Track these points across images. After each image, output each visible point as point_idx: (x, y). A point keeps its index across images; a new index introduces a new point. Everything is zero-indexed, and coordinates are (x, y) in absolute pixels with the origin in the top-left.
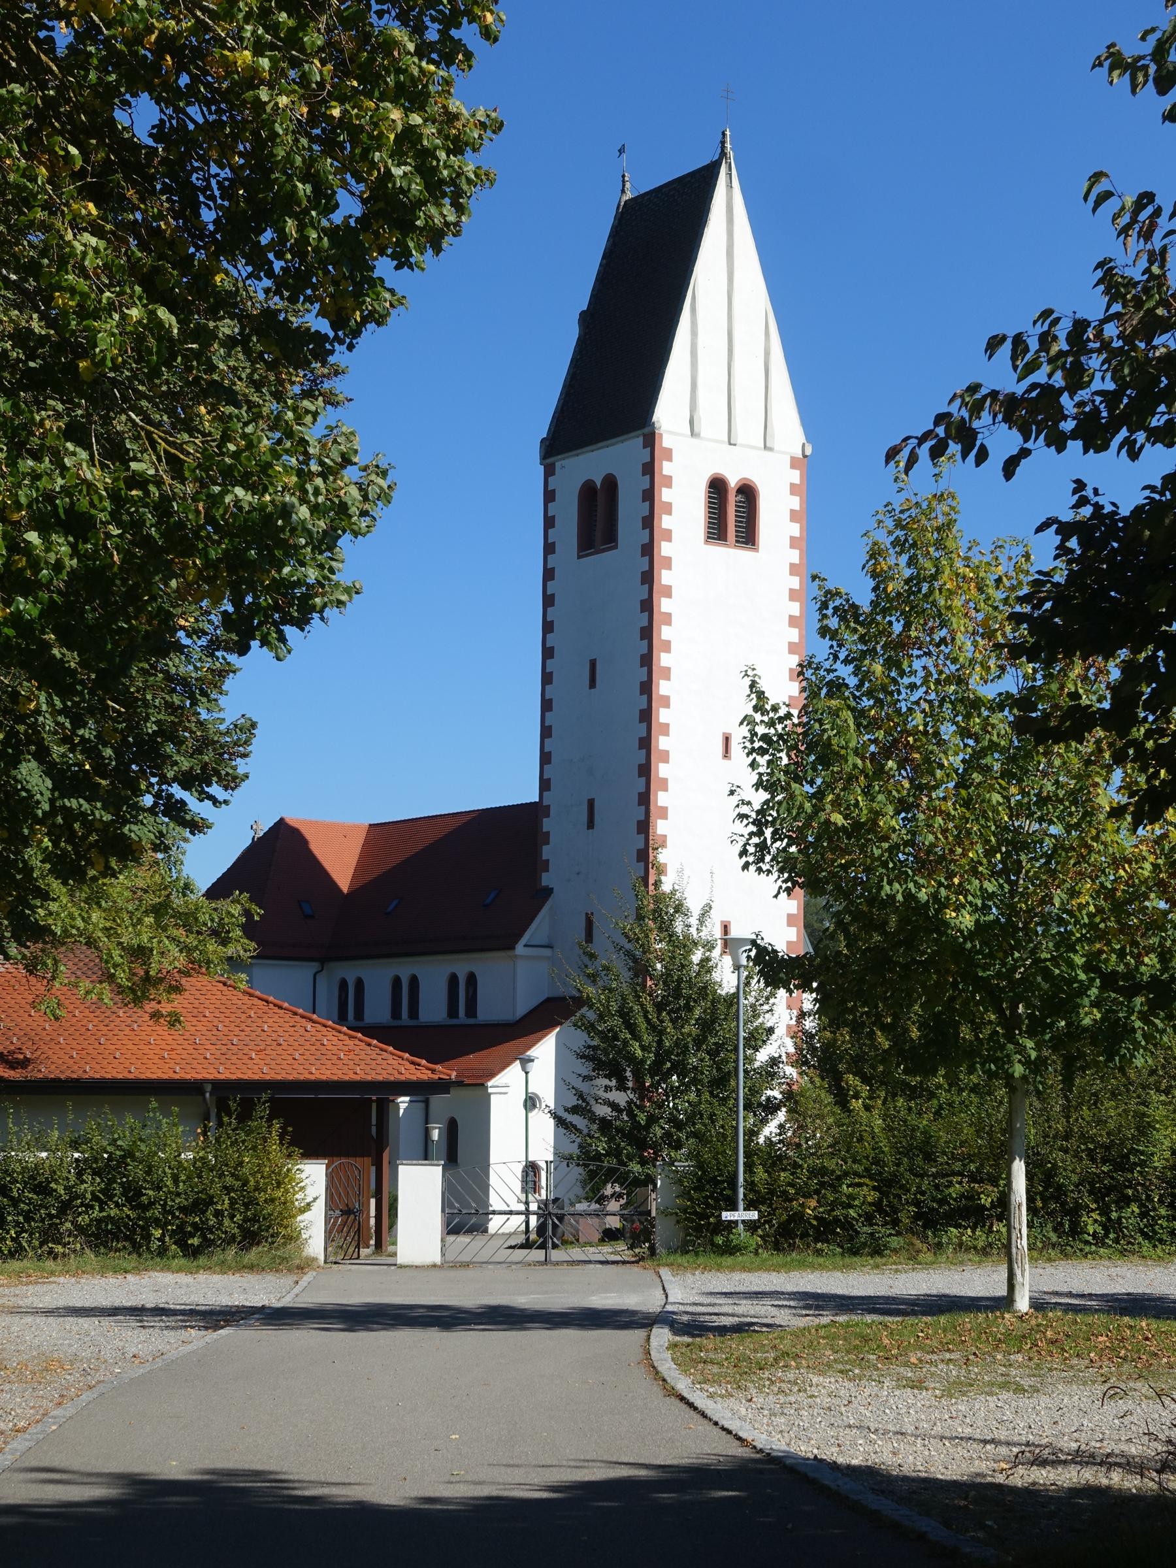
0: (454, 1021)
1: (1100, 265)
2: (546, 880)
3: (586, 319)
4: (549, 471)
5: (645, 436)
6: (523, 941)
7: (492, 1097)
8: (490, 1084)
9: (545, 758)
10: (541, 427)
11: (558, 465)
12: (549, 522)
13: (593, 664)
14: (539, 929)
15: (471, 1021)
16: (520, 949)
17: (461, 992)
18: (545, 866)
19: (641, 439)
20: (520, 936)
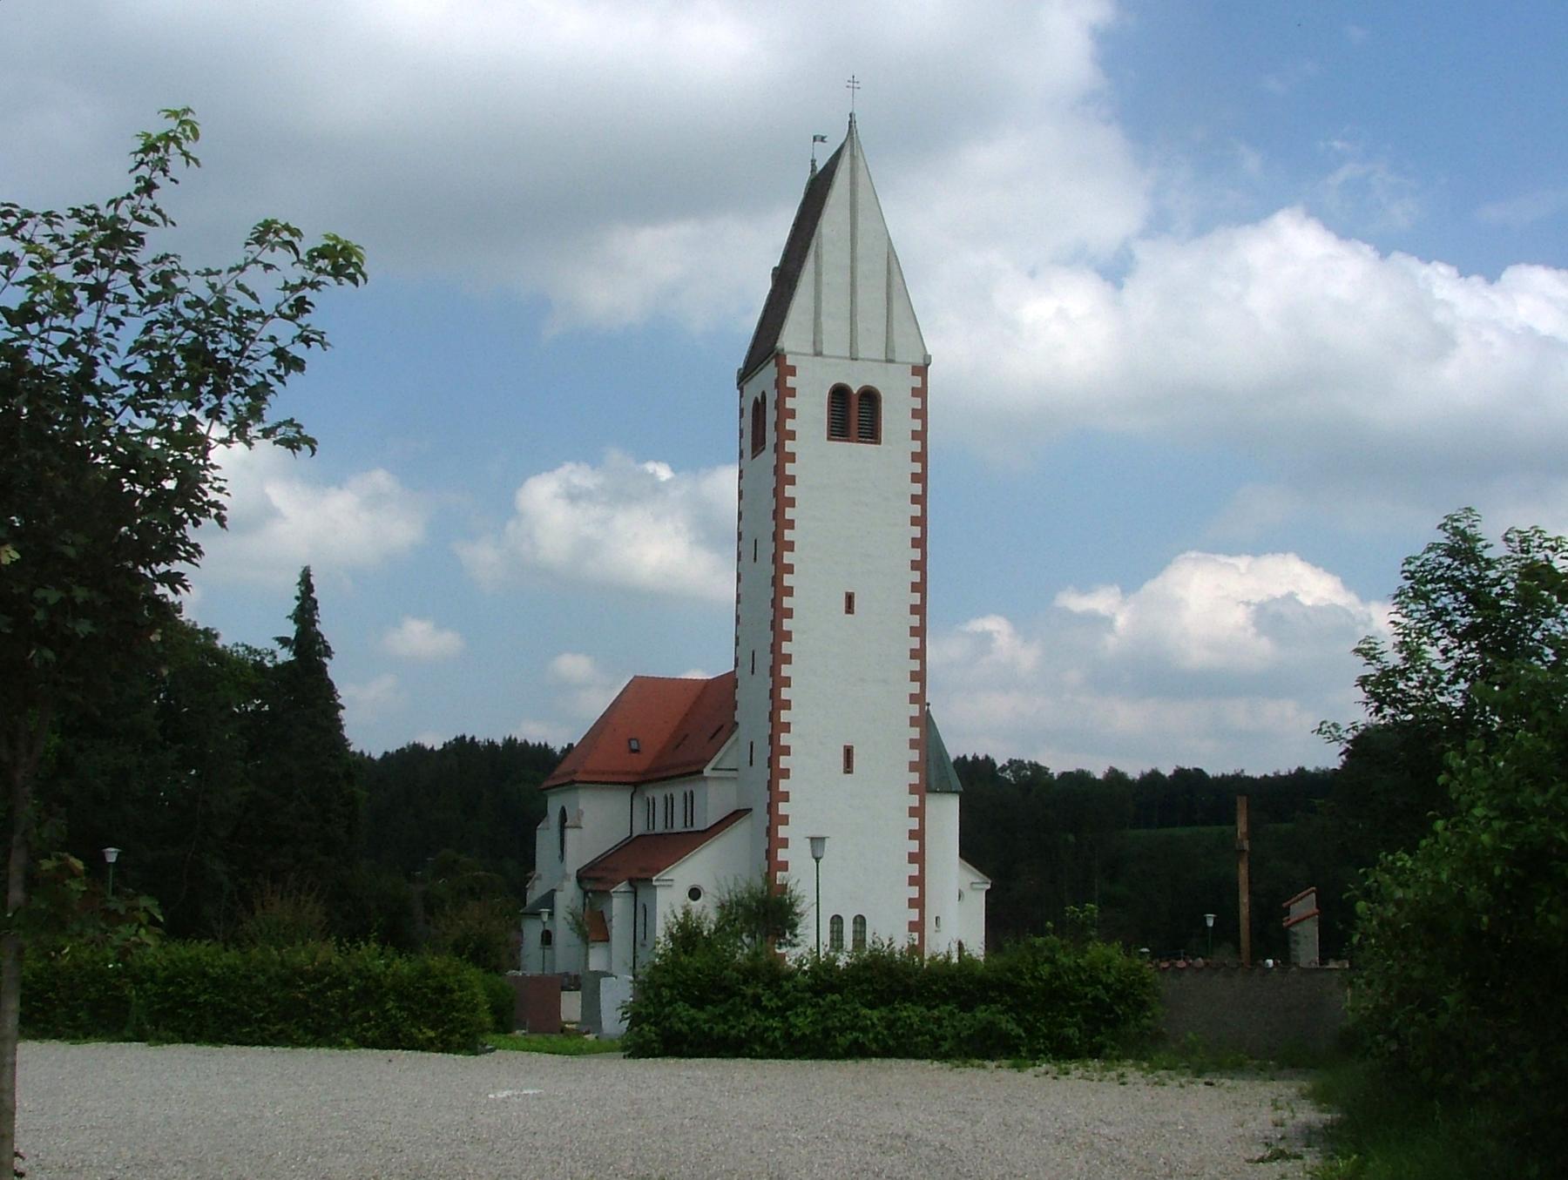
4: (741, 390)
6: (710, 766)
7: (659, 891)
16: (707, 771)
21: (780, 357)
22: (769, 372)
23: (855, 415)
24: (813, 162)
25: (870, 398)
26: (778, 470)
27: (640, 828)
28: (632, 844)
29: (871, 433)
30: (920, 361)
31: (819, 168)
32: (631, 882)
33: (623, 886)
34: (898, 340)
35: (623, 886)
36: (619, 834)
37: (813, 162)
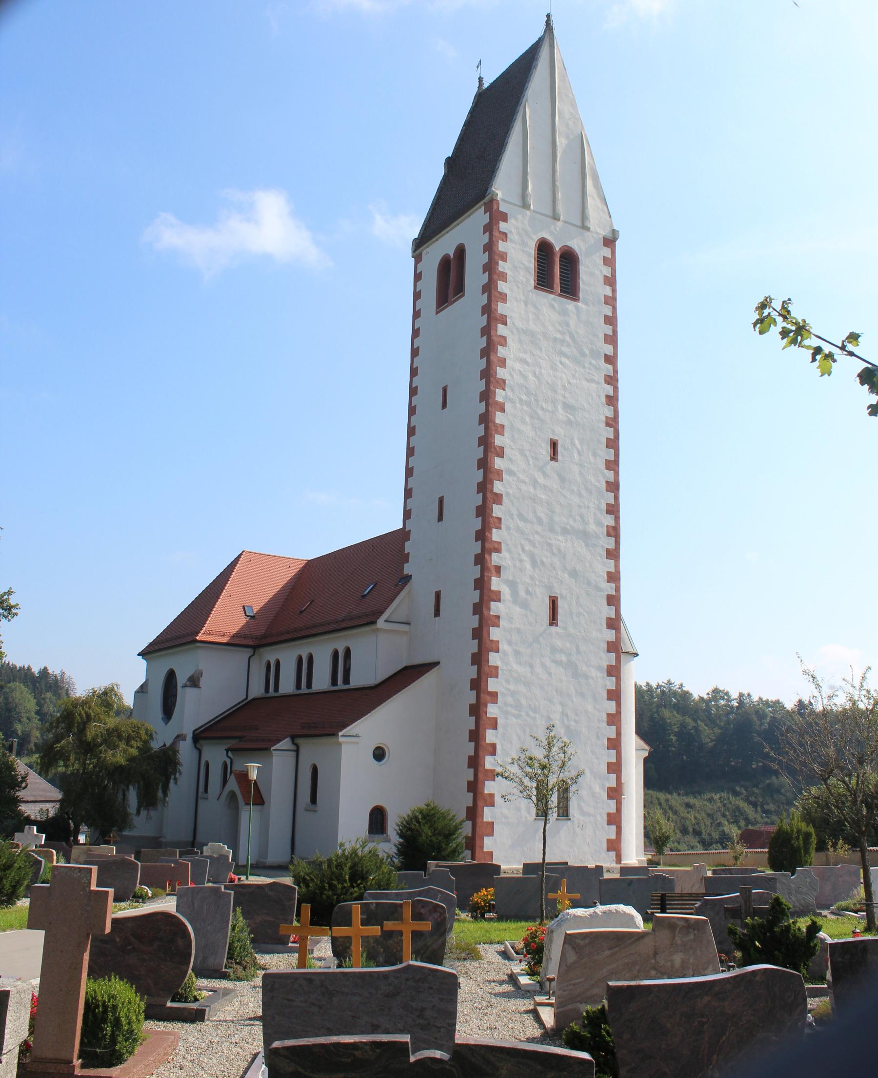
1: (762, 324)
2: (407, 569)
3: (450, 163)
4: (418, 258)
5: (485, 204)
6: (385, 616)
8: (340, 734)
9: (409, 472)
12: (417, 296)
14: (397, 608)
15: (346, 687)
16: (381, 623)
18: (406, 558)
19: (483, 208)
20: (381, 613)
22: (478, 217)
23: (557, 270)
24: (480, 80)
25: (570, 259)
26: (488, 310)
29: (570, 288)
30: (610, 236)
31: (486, 85)
32: (293, 738)
33: (285, 744)
35: (285, 744)
36: (235, 698)
37: (480, 80)
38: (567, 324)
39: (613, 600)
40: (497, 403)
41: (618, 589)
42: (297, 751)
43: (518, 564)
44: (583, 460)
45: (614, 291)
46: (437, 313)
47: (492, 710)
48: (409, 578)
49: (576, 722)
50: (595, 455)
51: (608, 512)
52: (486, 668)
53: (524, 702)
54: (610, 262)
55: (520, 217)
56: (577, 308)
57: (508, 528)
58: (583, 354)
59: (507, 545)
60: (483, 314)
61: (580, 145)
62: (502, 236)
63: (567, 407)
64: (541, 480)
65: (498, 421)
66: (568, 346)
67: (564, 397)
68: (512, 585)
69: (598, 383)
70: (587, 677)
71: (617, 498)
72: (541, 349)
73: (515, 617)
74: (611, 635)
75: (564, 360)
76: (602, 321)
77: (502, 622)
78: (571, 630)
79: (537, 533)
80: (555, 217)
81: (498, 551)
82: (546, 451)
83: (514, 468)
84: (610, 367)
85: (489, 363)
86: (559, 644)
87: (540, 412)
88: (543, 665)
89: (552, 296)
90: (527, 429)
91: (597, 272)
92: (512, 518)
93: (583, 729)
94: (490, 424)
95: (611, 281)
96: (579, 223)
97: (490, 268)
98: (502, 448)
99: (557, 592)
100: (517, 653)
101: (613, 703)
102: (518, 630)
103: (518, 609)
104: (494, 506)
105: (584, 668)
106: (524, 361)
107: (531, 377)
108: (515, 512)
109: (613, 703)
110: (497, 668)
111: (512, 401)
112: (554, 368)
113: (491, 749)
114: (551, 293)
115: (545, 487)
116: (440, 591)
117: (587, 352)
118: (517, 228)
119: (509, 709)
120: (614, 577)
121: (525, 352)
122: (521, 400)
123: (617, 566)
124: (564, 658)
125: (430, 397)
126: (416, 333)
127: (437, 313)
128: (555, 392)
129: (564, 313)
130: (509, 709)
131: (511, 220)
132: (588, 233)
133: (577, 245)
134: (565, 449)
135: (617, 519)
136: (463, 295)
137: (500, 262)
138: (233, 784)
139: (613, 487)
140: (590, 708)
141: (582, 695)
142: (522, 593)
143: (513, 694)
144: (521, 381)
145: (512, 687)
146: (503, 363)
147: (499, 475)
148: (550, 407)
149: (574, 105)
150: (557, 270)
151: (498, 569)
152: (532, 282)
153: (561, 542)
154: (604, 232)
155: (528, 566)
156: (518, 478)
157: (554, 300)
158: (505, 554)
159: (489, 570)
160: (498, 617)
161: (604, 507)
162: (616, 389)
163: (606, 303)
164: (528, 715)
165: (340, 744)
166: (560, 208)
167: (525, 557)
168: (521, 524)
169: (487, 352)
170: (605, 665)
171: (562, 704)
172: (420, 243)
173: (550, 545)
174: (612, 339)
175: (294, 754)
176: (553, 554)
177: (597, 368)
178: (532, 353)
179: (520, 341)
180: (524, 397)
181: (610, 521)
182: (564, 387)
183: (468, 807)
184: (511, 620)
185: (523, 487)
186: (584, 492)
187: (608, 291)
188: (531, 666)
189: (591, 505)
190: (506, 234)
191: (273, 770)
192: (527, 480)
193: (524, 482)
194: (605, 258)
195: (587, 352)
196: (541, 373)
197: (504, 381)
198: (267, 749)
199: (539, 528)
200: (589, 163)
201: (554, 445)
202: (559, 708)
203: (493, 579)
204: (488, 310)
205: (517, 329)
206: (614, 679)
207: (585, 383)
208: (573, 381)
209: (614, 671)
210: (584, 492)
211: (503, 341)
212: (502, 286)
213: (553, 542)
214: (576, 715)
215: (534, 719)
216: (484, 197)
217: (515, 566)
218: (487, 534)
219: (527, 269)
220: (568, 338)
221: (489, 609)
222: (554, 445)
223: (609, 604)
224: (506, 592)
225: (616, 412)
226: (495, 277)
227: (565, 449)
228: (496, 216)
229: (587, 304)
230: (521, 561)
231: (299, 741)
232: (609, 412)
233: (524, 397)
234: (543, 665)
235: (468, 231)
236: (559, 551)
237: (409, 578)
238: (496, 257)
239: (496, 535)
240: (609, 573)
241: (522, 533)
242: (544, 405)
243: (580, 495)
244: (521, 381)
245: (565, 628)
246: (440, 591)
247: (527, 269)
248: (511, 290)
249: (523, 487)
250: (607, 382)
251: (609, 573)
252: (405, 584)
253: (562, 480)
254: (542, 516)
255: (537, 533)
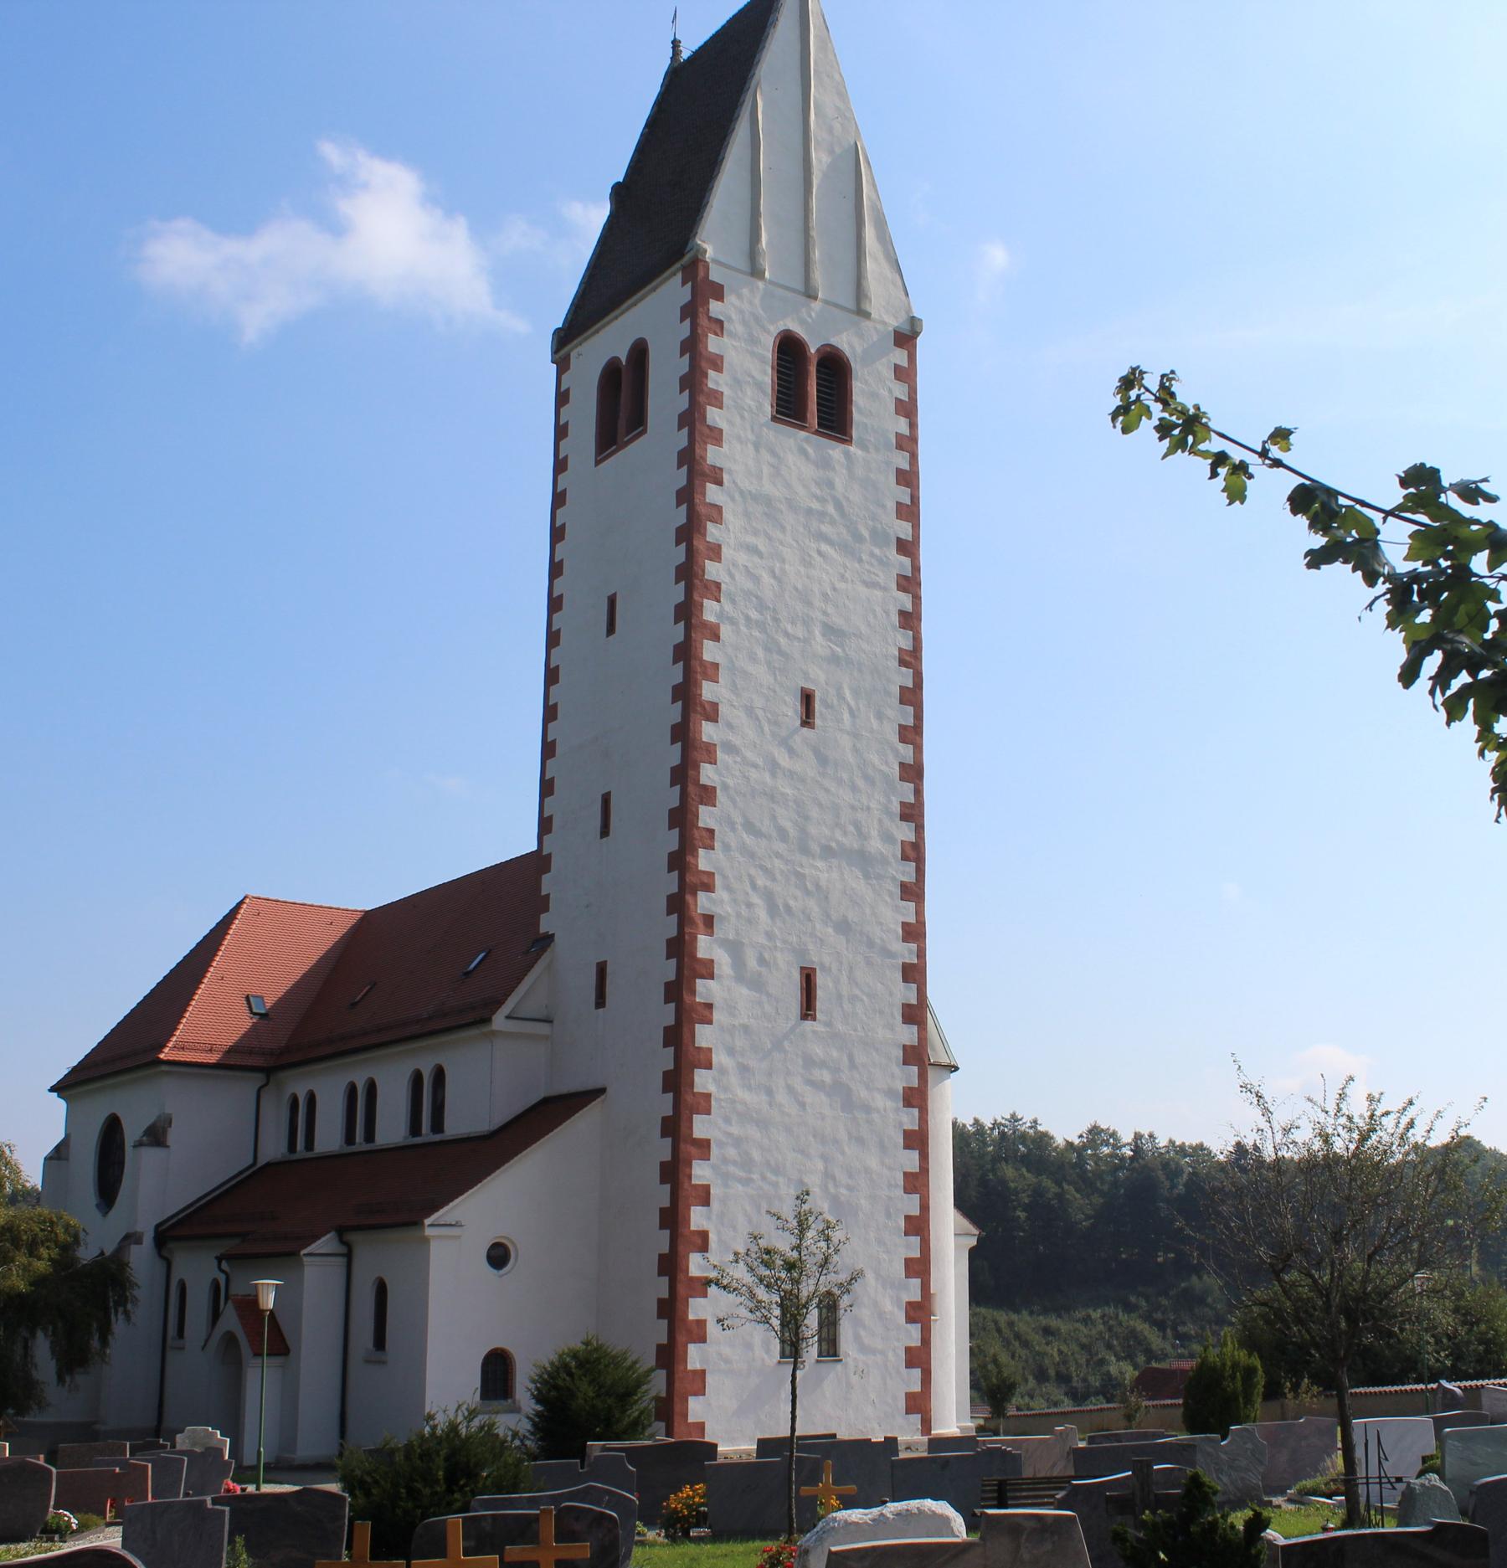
0: (418, 1140)
2: (546, 923)
3: (620, 193)
4: (562, 365)
5: (684, 268)
7: (434, 1247)
8: (427, 1222)
9: (548, 750)
10: (557, 318)
11: (573, 355)
12: (561, 432)
13: (612, 601)
14: (529, 993)
15: (437, 1138)
16: (499, 1021)
17: (428, 1094)
18: (543, 904)
19: (679, 276)
20: (499, 1003)
21: (694, 270)
22: (672, 291)
23: (813, 389)
24: (675, 44)
25: (835, 368)
26: (688, 457)
27: (274, 1148)
28: (256, 1180)
29: (835, 421)
30: (906, 329)
31: (685, 55)
32: (341, 1232)
34: (873, 285)
37: (675, 44)
38: (830, 485)
39: (914, 973)
40: (706, 625)
41: (921, 954)
42: (349, 1256)
43: (744, 911)
44: (859, 727)
45: (913, 426)
46: (598, 463)
47: (701, 1172)
48: (549, 938)
49: (850, 1188)
50: (880, 716)
51: (905, 817)
52: (689, 1098)
53: (756, 1155)
54: (906, 375)
55: (745, 291)
56: (847, 455)
57: (727, 848)
58: (859, 538)
59: (725, 877)
60: (680, 466)
61: (853, 164)
62: (714, 326)
63: (830, 631)
64: (783, 760)
65: (707, 657)
66: (833, 523)
67: (825, 613)
68: (735, 949)
69: (885, 589)
70: (867, 1109)
71: (918, 792)
72: (783, 529)
73: (738, 1006)
74: (909, 1034)
75: (825, 547)
76: (893, 478)
77: (716, 1015)
78: (840, 1027)
79: (778, 855)
80: (810, 294)
81: (709, 888)
82: (791, 710)
83: (736, 740)
84: (907, 561)
85: (690, 553)
86: (818, 1051)
87: (783, 641)
88: (791, 1090)
89: (803, 434)
90: (760, 672)
91: (885, 393)
92: (733, 829)
93: (863, 1201)
94: (693, 662)
95: (907, 409)
96: (851, 305)
97: (692, 382)
98: (715, 706)
99: (814, 958)
100: (744, 1069)
101: (915, 1155)
102: (746, 1029)
103: (745, 991)
104: (702, 808)
105: (864, 1094)
106: (753, 550)
107: (766, 578)
108: (739, 820)
109: (915, 1155)
110: (708, 1096)
111: (733, 622)
112: (807, 563)
113: (699, 1242)
114: (802, 428)
115: (791, 774)
116: (605, 962)
117: (866, 533)
118: (741, 312)
119: (732, 1168)
120: (914, 933)
121: (756, 533)
122: (748, 618)
123: (920, 913)
124: (827, 1077)
125: (585, 614)
126: (559, 499)
127: (598, 463)
128: (809, 604)
129: (825, 464)
130: (732, 1168)
131: (730, 298)
132: (867, 323)
133: (847, 343)
134: (828, 706)
135: (920, 829)
136: (644, 432)
137: (711, 373)
138: (230, 1320)
139: (913, 772)
140: (873, 1162)
141: (860, 1141)
142: (752, 963)
143: (738, 1142)
144: (749, 585)
145: (735, 1130)
146: (715, 552)
147: (710, 753)
148: (799, 631)
149: (842, 95)
150: (813, 389)
151: (709, 920)
152: (768, 409)
153: (821, 871)
154: (894, 322)
155: (762, 914)
156: (744, 758)
157: (807, 440)
158: (720, 893)
159: (693, 922)
160: (710, 1006)
161: (896, 808)
162: (917, 599)
163: (900, 447)
164: (764, 1178)
165: (426, 1241)
166: (818, 277)
167: (756, 899)
168: (749, 840)
169: (688, 533)
170: (899, 1086)
171: (825, 1159)
172: (566, 339)
173: (801, 876)
174: (910, 512)
175: (342, 1260)
176: (808, 893)
177: (884, 563)
178: (770, 539)
179: (747, 515)
180: (754, 615)
181: (906, 832)
182: (825, 595)
183: (659, 1346)
184: (732, 1010)
185: (753, 774)
186: (861, 783)
187: (902, 426)
188: (769, 1092)
189: (873, 805)
190: (720, 323)
191: (303, 1292)
192: (760, 762)
193: (755, 766)
194: (897, 368)
195: (866, 533)
196: (783, 571)
197: (718, 585)
198: (293, 1254)
199: (780, 847)
200: (869, 198)
201: (807, 699)
202: (820, 1165)
203: (701, 937)
204: (688, 457)
205: (742, 493)
206: (916, 1111)
207: (862, 589)
208: (841, 585)
209: (916, 1098)
210: (861, 783)
211: (717, 514)
212: (714, 416)
213: (807, 871)
214: (851, 1176)
215: (775, 1185)
216: (683, 255)
217: (739, 915)
218: (689, 858)
219: (759, 386)
220: (831, 509)
221: (693, 992)
222: (807, 699)
223: (906, 979)
224: (723, 961)
225: (917, 641)
226: (702, 399)
227: (828, 706)
228: (704, 291)
229: (864, 448)
230: (749, 905)
231: (352, 1237)
232: (904, 640)
233: (754, 615)
234: (791, 1090)
235: (653, 315)
236: (818, 886)
237: (549, 938)
238: (704, 364)
239: (704, 861)
240: (905, 925)
241: (752, 855)
242: (789, 628)
243: (854, 788)
244: (749, 585)
245: (829, 1024)
246: (605, 962)
247: (759, 386)
248: (730, 422)
249: (753, 774)
250: (901, 588)
251: (905, 925)
252: (544, 950)
253: (823, 760)
254: (788, 825)
255: (778, 855)
